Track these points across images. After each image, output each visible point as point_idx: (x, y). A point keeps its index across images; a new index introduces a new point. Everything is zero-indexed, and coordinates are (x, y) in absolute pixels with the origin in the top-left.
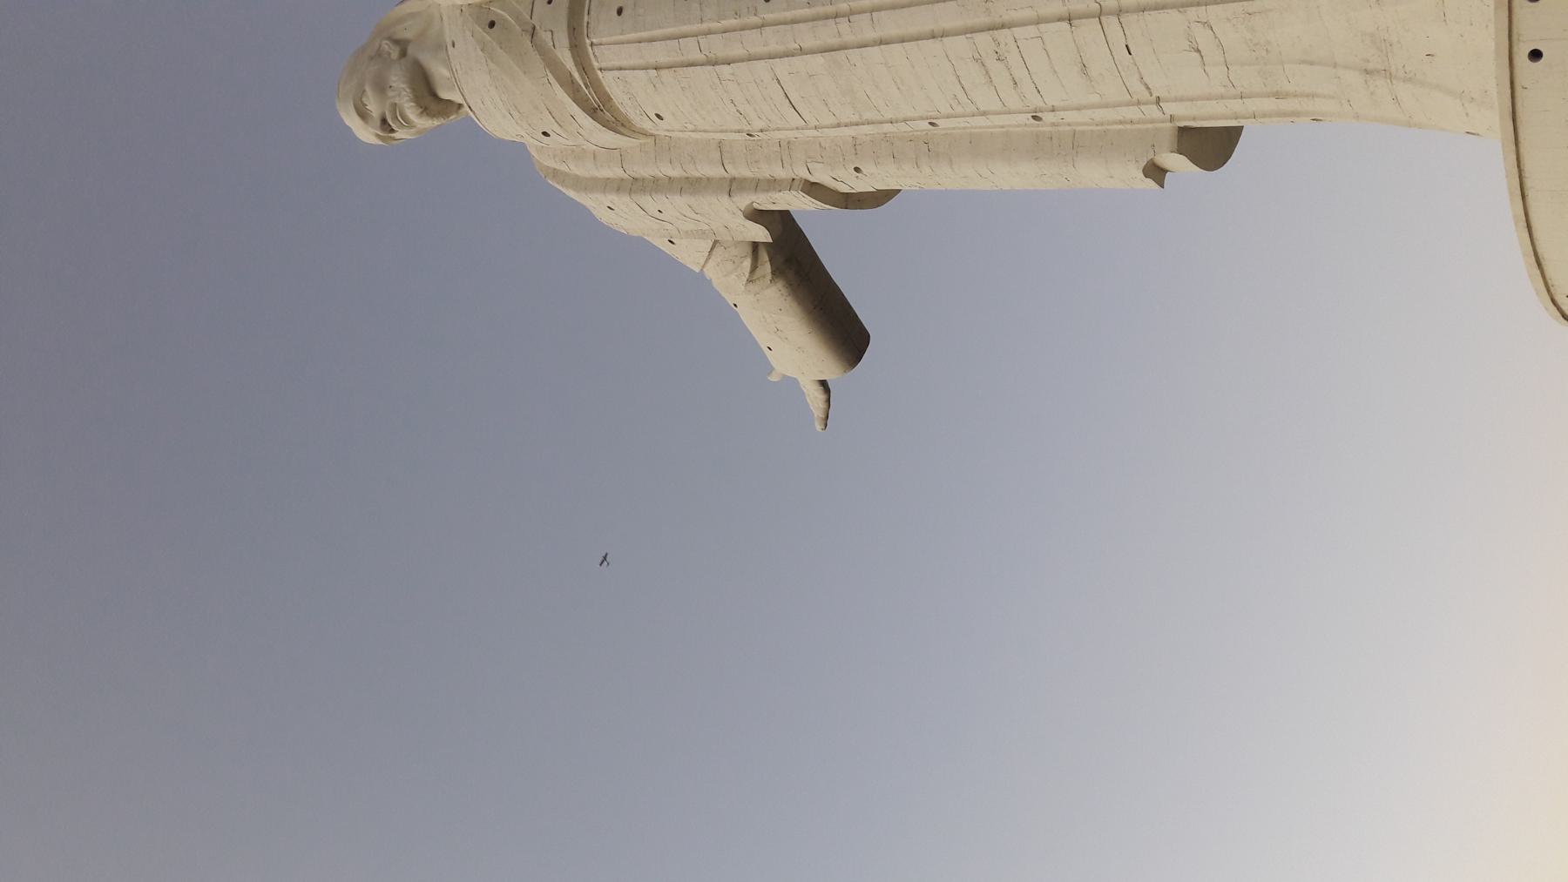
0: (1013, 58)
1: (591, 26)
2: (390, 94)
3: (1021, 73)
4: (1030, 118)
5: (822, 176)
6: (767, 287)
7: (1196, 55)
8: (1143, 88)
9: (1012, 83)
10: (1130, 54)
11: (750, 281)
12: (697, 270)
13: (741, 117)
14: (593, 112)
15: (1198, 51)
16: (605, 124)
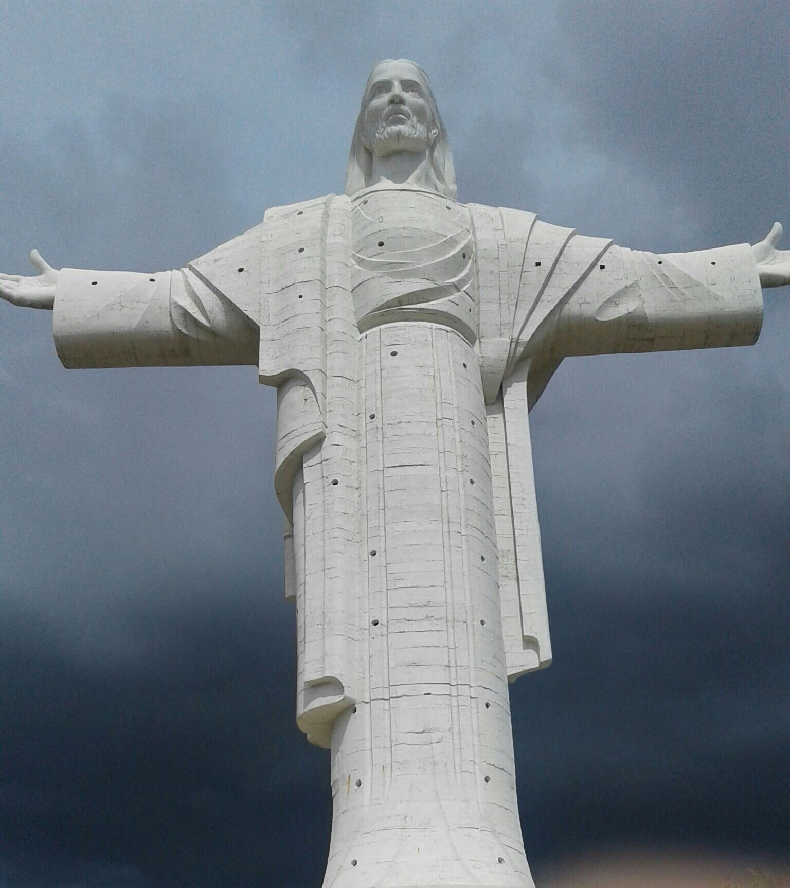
0: (426, 625)
1: (457, 337)
2: (415, 119)
3: (416, 626)
4: (376, 619)
5: (327, 450)
7: (421, 731)
8: (399, 695)
9: (410, 619)
10: (425, 694)
11: (186, 314)
12: (191, 263)
13: (396, 422)
14: (401, 301)
15: (422, 733)
16: (388, 305)
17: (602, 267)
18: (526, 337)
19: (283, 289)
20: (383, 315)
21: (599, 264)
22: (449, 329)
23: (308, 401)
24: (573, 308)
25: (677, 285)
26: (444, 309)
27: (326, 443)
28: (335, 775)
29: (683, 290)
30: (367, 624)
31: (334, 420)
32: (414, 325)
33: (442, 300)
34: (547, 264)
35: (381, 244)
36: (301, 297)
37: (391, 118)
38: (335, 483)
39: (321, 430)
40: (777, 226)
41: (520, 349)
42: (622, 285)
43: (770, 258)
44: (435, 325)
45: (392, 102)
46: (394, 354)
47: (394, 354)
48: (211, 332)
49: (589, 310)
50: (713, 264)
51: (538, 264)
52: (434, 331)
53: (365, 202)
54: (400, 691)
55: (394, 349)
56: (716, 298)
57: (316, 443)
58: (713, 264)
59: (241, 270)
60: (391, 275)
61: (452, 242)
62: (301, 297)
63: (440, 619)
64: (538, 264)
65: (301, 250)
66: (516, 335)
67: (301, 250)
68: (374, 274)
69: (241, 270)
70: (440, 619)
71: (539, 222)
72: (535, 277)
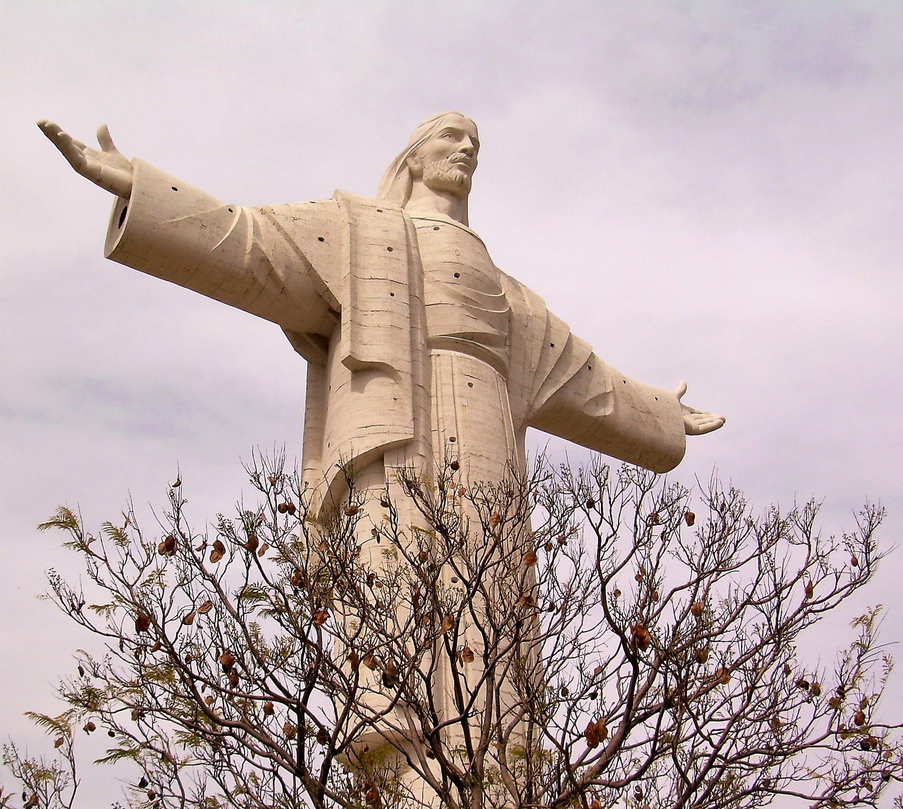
14: (473, 336)
16: (463, 335)
18: (537, 406)
19: (371, 278)
20: (457, 342)
23: (398, 401)
24: (570, 395)
27: (410, 450)
32: (486, 366)
33: (501, 350)
34: (559, 348)
36: (392, 295)
37: (459, 163)
39: (412, 436)
41: (531, 414)
45: (464, 151)
46: (470, 385)
48: (283, 290)
49: (581, 401)
53: (436, 229)
55: (472, 381)
59: (321, 240)
60: (470, 309)
65: (390, 249)
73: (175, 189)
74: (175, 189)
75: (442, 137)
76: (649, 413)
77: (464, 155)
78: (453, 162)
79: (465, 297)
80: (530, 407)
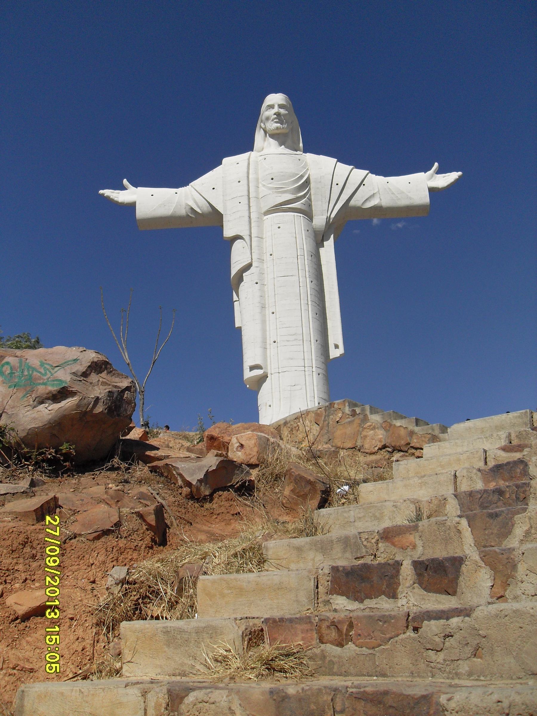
6: (186, 213)
11: (192, 209)
14: (281, 204)
16: (276, 206)
17: (364, 185)
18: (333, 215)
21: (363, 183)
22: (302, 215)
24: (352, 203)
25: (394, 192)
26: (299, 207)
28: (260, 402)
29: (397, 195)
30: (272, 342)
31: (255, 257)
35: (272, 179)
38: (257, 283)
40: (436, 164)
42: (372, 193)
43: (433, 178)
44: (296, 214)
45: (275, 114)
46: (279, 228)
47: (279, 228)
48: (202, 215)
50: (409, 183)
51: (337, 184)
52: (295, 217)
53: (265, 159)
54: (285, 369)
56: (410, 198)
57: (248, 267)
58: (409, 183)
59: (214, 189)
61: (302, 177)
62: (240, 203)
63: (300, 340)
64: (337, 184)
65: (239, 182)
66: (329, 215)
67: (239, 182)
68: (270, 192)
69: (214, 189)
70: (300, 340)
71: (338, 163)
72: (336, 190)
73: (152, 195)
74: (152, 195)
75: (267, 110)
76: (403, 193)
77: (275, 116)
78: (273, 120)
79: (276, 188)
80: (328, 219)
